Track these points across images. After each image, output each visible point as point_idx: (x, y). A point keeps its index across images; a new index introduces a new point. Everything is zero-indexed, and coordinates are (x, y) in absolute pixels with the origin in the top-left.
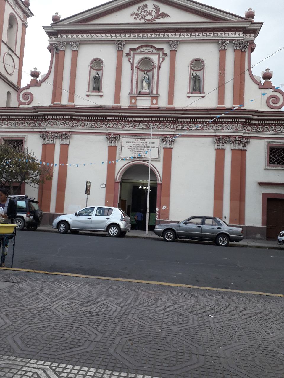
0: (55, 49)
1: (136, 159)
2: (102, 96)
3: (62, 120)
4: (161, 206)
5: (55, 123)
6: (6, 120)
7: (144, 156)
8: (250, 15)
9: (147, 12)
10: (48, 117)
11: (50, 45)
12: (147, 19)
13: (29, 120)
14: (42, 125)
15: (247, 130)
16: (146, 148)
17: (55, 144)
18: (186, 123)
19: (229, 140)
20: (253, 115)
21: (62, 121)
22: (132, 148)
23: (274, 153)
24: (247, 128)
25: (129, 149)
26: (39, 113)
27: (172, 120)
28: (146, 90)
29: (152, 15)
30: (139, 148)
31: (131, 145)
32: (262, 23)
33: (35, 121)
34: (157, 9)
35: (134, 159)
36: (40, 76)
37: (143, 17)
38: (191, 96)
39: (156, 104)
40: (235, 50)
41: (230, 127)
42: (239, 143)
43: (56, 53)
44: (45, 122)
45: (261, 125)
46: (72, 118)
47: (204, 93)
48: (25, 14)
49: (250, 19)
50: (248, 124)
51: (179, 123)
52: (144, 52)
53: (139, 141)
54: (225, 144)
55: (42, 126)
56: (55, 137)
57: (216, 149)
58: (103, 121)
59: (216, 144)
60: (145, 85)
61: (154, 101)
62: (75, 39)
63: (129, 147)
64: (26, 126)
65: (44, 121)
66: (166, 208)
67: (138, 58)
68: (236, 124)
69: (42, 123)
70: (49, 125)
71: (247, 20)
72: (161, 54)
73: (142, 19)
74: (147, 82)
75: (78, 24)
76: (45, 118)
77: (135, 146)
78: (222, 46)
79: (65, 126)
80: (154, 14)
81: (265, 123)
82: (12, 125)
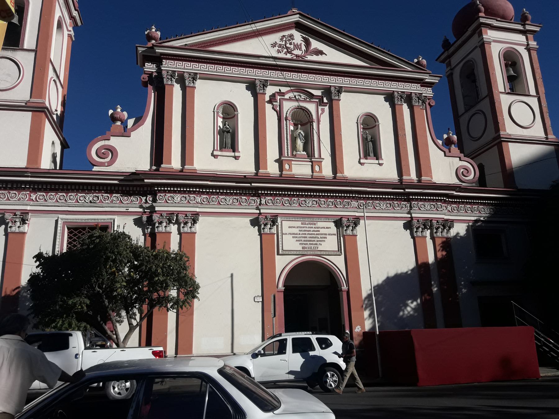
1: (306, 253)
9: (294, 45)
12: (296, 54)
16: (319, 236)
25: (293, 237)
29: (300, 49)
30: (308, 236)
31: (296, 231)
34: (308, 44)
37: (290, 50)
38: (366, 163)
41: (427, 206)
47: (382, 160)
53: (308, 226)
56: (173, 221)
60: (300, 144)
61: (317, 168)
63: (294, 234)
67: (288, 107)
68: (434, 202)
69: (145, 198)
70: (159, 201)
71: (427, 71)
77: (304, 232)
80: (304, 48)
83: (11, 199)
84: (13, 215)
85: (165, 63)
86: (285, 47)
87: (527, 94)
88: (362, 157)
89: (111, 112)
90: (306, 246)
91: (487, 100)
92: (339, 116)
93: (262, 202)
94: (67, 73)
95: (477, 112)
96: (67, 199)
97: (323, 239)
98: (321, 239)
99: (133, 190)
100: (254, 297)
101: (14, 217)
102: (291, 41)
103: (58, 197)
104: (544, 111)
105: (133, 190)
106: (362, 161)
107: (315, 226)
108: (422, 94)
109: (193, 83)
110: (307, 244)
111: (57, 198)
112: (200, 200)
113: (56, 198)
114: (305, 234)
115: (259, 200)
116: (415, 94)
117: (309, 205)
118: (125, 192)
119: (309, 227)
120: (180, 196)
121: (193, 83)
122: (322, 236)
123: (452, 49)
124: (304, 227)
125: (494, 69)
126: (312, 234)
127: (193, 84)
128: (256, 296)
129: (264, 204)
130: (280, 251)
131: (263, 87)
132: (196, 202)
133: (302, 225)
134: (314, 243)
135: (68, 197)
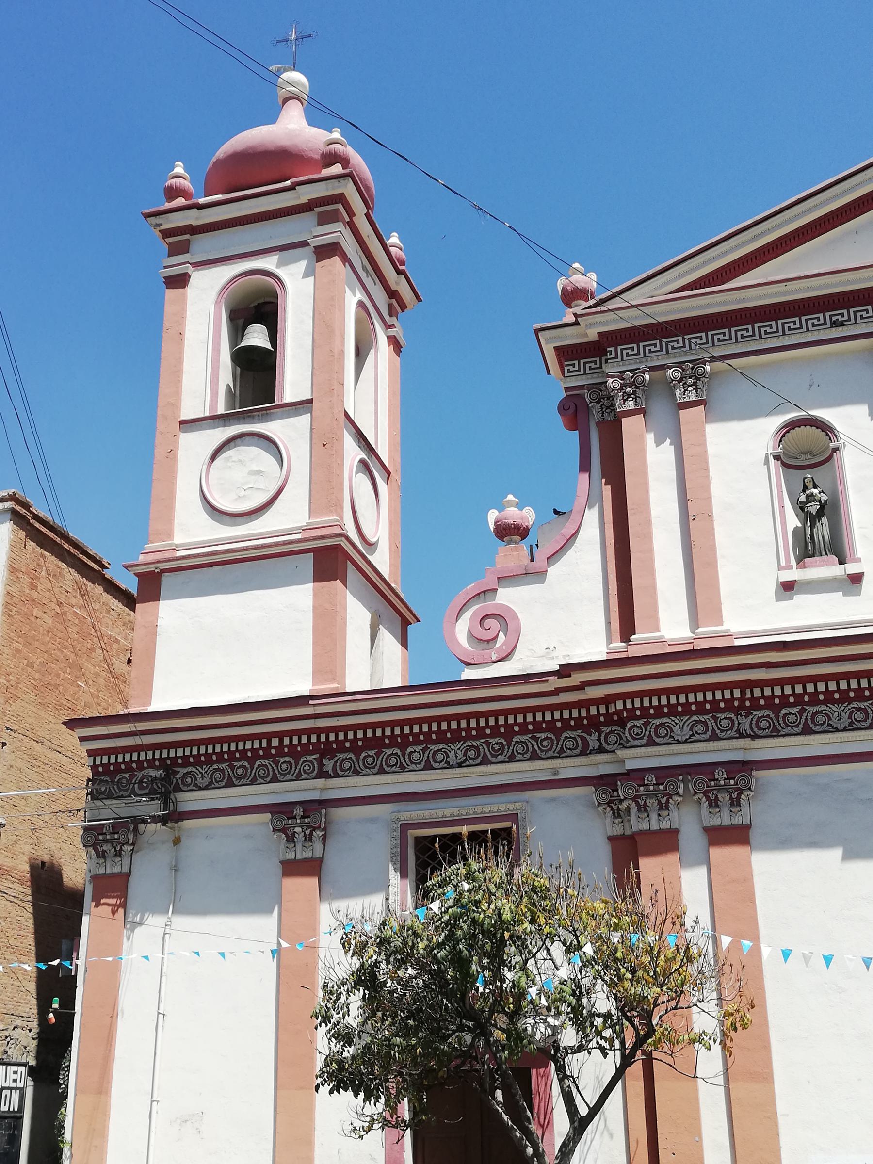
0: (598, 408)
3: (698, 712)
5: (662, 731)
6: (417, 742)
10: (629, 705)
13: (529, 732)
17: (677, 831)
21: (695, 718)
33: (558, 732)
43: (598, 424)
44: (612, 732)
46: (748, 696)
48: (394, 301)
56: (676, 798)
64: (518, 757)
65: (607, 724)
69: (595, 736)
70: (633, 743)
76: (612, 709)
79: (714, 737)
83: (281, 778)
84: (289, 819)
85: (613, 355)
89: (493, 516)
94: (397, 432)
96: (405, 761)
99: (562, 719)
101: (290, 822)
103: (384, 760)
105: (562, 719)
111: (382, 761)
112: (747, 727)
113: (379, 762)
118: (544, 726)
120: (689, 721)
121: (696, 389)
127: (697, 391)
132: (738, 731)
135: (407, 757)
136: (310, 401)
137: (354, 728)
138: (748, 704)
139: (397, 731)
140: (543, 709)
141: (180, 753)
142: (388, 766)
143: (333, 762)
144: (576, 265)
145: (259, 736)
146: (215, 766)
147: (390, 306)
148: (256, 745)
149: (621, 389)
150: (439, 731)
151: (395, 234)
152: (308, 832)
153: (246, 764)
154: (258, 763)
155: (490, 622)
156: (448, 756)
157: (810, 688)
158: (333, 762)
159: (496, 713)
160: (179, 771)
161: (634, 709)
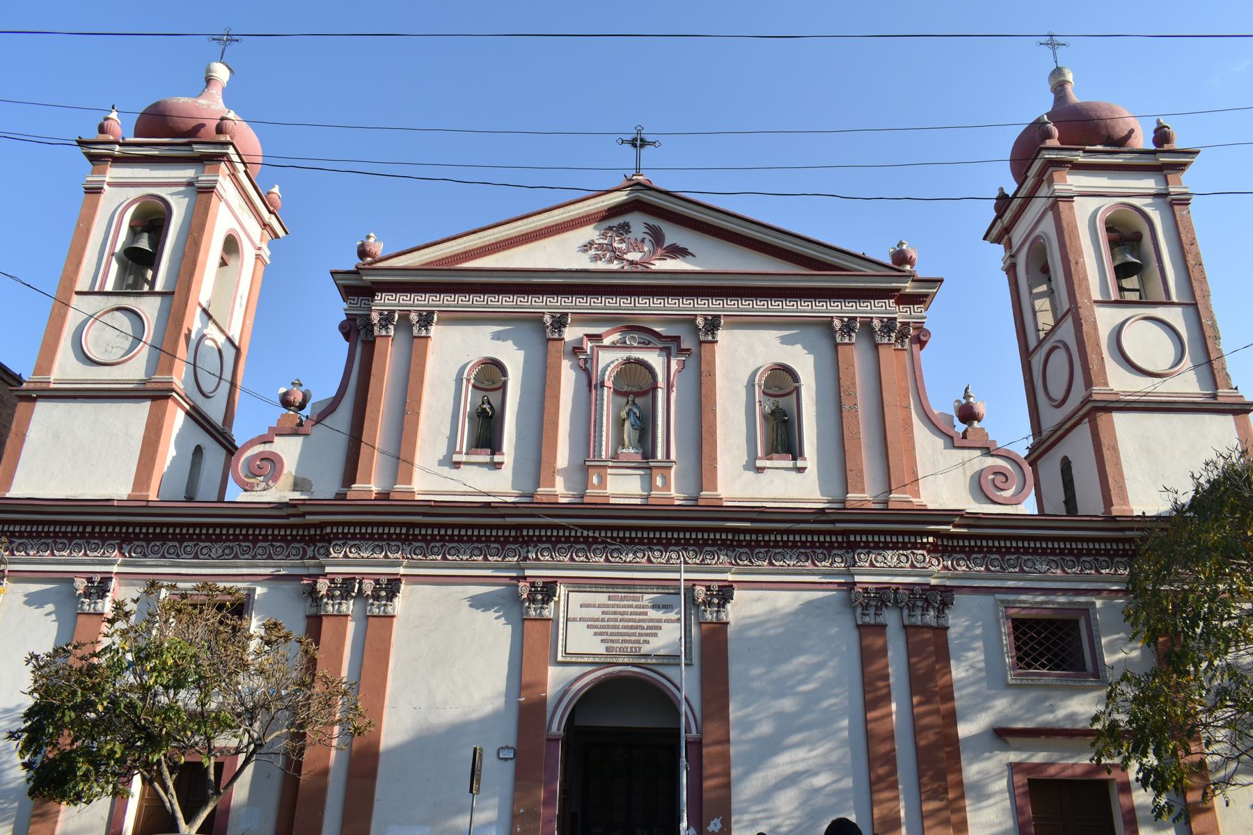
1: (614, 660)
2: (502, 463)
4: (704, 822)
6: (191, 539)
7: (640, 648)
8: (901, 258)
10: (335, 531)
11: (348, 319)
12: (631, 259)
13: (268, 541)
14: (310, 553)
15: (941, 565)
16: (645, 625)
18: (764, 547)
19: (895, 599)
20: (955, 526)
21: (376, 543)
22: (600, 623)
23: (1024, 633)
24: (939, 564)
25: (588, 627)
26: (308, 517)
27: (721, 539)
28: (630, 452)
30: (621, 624)
31: (596, 613)
32: (941, 281)
33: (288, 543)
34: (657, 237)
35: (609, 660)
36: (309, 406)
39: (666, 485)
40: (876, 346)
42: (925, 606)
43: (363, 341)
45: (978, 552)
46: (411, 532)
48: (265, 232)
49: (908, 267)
50: (940, 548)
51: (741, 547)
52: (625, 345)
54: (884, 609)
55: (310, 558)
57: (858, 627)
58: (507, 540)
59: (859, 610)
61: (659, 481)
62: (424, 306)
64: (259, 557)
65: (320, 541)
66: (719, 826)
67: (608, 361)
72: (674, 350)
73: (616, 258)
74: (636, 427)
75: (435, 267)
76: (324, 532)
77: (613, 616)
78: (843, 336)
81: (988, 547)
82: (210, 556)
85: (379, 298)
86: (611, 249)
87: (1165, 300)
88: (759, 455)
89: (283, 390)
90: (615, 645)
91: (1070, 319)
92: (712, 374)
93: (530, 555)
94: (249, 322)
95: (1055, 344)
97: (654, 631)
98: (649, 631)
99: (291, 535)
100: (499, 750)
102: (623, 237)
104: (1207, 335)
105: (291, 535)
106: (759, 463)
107: (637, 603)
108: (895, 319)
109: (427, 329)
110: (617, 641)
114: (616, 620)
115: (525, 550)
116: (881, 319)
117: (628, 560)
119: (624, 606)
121: (427, 329)
122: (651, 624)
123: (1008, 215)
124: (613, 606)
125: (1081, 254)
126: (629, 620)
128: (502, 748)
129: (534, 557)
130: (560, 654)
131: (560, 327)
133: (609, 600)
134: (633, 638)
136: (172, 293)
137: (148, 525)
138: (411, 537)
139: (178, 531)
140: (279, 526)
141: (17, 529)
142: (168, 553)
143: (129, 547)
144: (372, 234)
145: (78, 523)
146: (43, 541)
147: (262, 234)
148: (75, 529)
149: (379, 321)
150: (207, 534)
151: (277, 186)
152: (101, 594)
153: (66, 542)
154: (75, 542)
155: (264, 462)
156: (211, 551)
157: (449, 532)
158: (129, 547)
159: (248, 526)
160: (14, 542)
161: (337, 533)
